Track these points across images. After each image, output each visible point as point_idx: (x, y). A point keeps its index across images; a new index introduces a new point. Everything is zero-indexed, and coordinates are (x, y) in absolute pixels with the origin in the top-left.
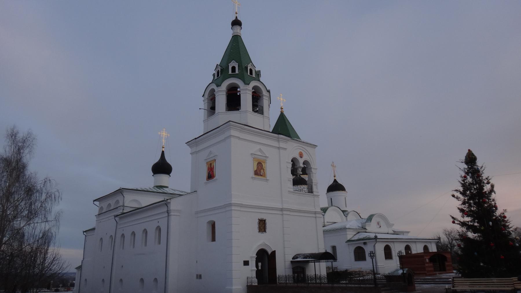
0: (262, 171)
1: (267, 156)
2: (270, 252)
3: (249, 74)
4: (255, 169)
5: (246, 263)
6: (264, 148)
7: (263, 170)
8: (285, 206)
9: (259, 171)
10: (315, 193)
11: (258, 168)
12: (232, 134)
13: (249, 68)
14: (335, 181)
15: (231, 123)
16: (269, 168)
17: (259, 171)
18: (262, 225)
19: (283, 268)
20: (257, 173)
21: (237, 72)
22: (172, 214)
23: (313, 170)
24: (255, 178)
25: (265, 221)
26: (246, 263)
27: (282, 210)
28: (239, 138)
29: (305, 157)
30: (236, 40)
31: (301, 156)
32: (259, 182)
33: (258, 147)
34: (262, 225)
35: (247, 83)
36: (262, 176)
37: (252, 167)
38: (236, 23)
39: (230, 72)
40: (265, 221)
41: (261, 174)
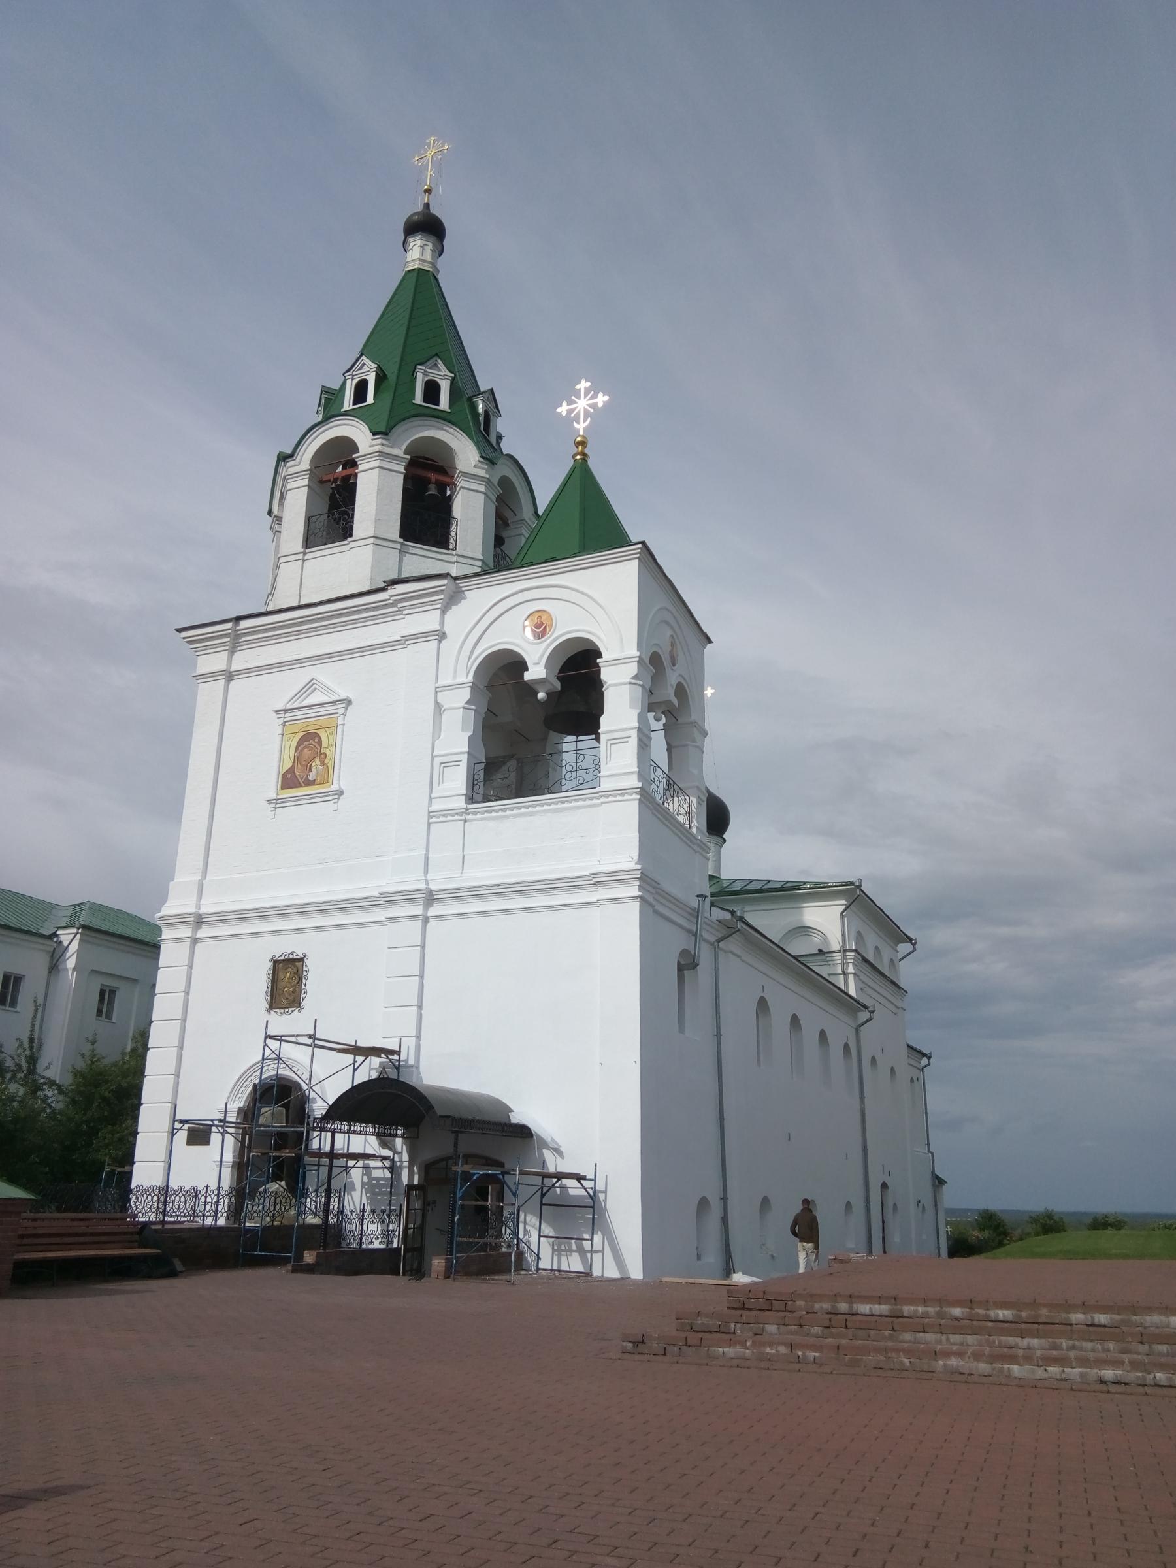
4: (287, 765)
5: (199, 1135)
6: (320, 673)
9: (306, 766)
10: (606, 785)
11: (298, 757)
17: (306, 766)
18: (286, 982)
20: (289, 780)
21: (444, 403)
25: (276, 962)
30: (422, 291)
34: (286, 982)
36: (312, 783)
38: (428, 226)
40: (276, 962)
41: (312, 777)
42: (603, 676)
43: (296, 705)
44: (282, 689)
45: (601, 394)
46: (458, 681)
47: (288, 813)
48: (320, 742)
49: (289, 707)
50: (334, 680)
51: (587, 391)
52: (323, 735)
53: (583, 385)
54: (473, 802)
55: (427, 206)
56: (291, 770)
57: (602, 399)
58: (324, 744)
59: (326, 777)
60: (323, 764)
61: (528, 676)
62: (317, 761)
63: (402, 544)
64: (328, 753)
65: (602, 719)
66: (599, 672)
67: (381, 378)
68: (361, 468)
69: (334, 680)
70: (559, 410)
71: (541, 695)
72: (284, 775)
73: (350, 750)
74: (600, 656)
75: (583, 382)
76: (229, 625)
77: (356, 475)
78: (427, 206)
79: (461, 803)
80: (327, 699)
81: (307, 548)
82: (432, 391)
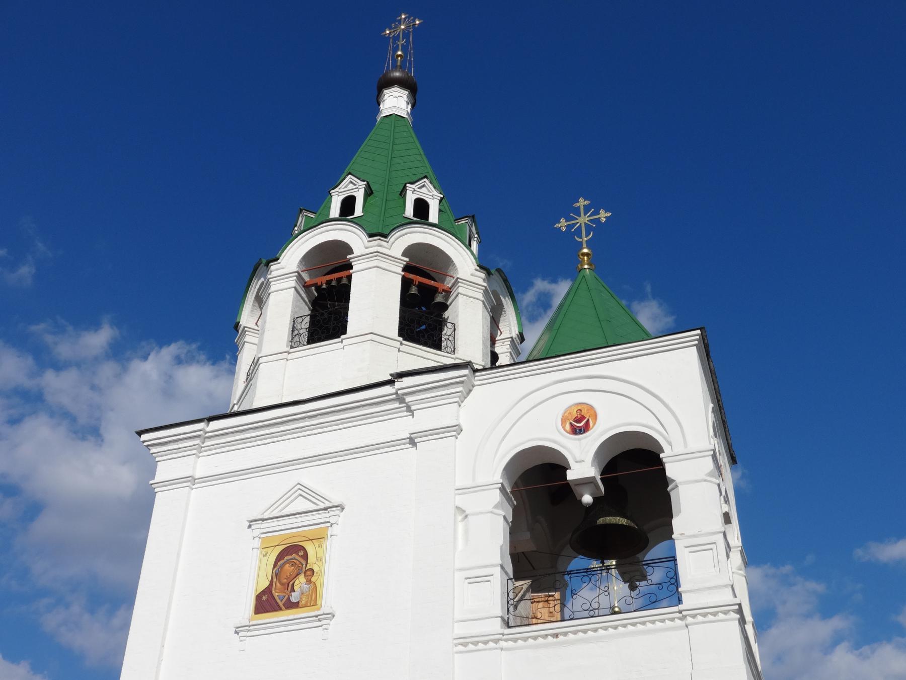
6: (309, 477)
9: (287, 584)
10: (689, 601)
17: (287, 584)
20: (266, 603)
28: (192, 480)
31: (579, 424)
36: (296, 605)
41: (294, 598)
42: (671, 471)
43: (275, 514)
44: (263, 495)
45: (602, 212)
46: (481, 480)
48: (306, 557)
49: (266, 516)
51: (587, 209)
52: (310, 548)
53: (582, 203)
54: (509, 627)
56: (268, 590)
57: (603, 215)
59: (312, 599)
60: (309, 582)
61: (571, 475)
62: (302, 579)
63: (401, 344)
64: (316, 569)
65: (675, 522)
66: (664, 470)
67: (369, 192)
68: (355, 269)
70: (558, 225)
71: (587, 499)
72: (259, 597)
73: (337, 569)
74: (663, 452)
75: (581, 200)
76: (201, 425)
77: (349, 278)
79: (496, 626)
81: (292, 347)
82: (421, 208)
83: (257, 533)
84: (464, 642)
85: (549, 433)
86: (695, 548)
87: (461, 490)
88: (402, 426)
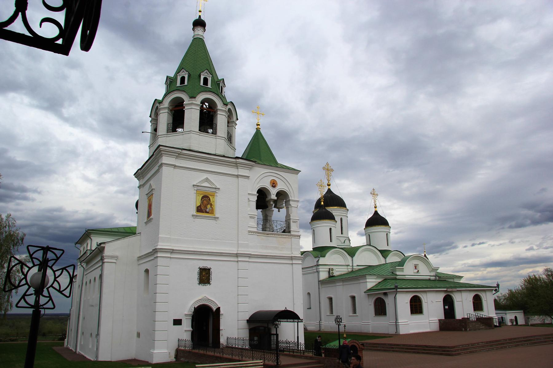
0: (209, 206)
1: (218, 187)
2: (214, 309)
3: (202, 83)
5: (178, 322)
6: (211, 177)
7: (211, 205)
8: (242, 251)
9: (205, 206)
10: (292, 233)
11: (202, 203)
12: (163, 162)
13: (202, 77)
14: (376, 213)
15: (161, 147)
16: (219, 203)
17: (205, 206)
18: (205, 276)
19: (233, 328)
20: (199, 209)
22: (105, 260)
23: (291, 203)
24: (196, 216)
26: (178, 322)
27: (237, 255)
28: (175, 166)
29: (281, 186)
31: (274, 185)
32: (204, 222)
33: (205, 176)
34: (205, 276)
35: (193, 97)
36: (208, 213)
37: (194, 201)
38: (199, 23)
39: (178, 84)
41: (208, 210)
47: (198, 220)
48: (210, 200)
50: (217, 181)
55: (200, 16)
56: (200, 206)
58: (211, 201)
59: (212, 212)
69: (217, 181)
72: (198, 207)
76: (180, 151)
78: (200, 16)
80: (210, 186)
83: (196, 189)
84: (249, 232)
85: (266, 184)
86: (294, 222)
87: (249, 194)
88: (233, 171)
